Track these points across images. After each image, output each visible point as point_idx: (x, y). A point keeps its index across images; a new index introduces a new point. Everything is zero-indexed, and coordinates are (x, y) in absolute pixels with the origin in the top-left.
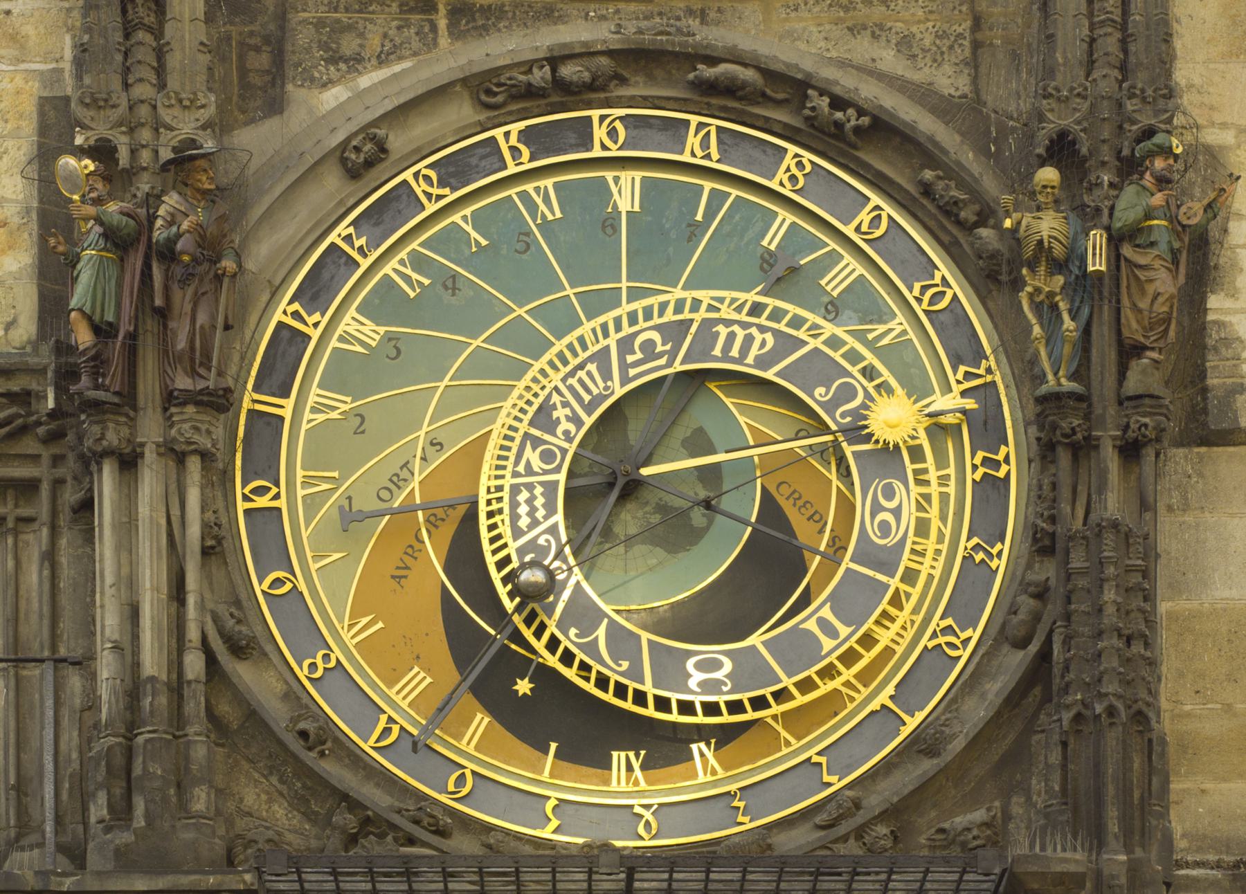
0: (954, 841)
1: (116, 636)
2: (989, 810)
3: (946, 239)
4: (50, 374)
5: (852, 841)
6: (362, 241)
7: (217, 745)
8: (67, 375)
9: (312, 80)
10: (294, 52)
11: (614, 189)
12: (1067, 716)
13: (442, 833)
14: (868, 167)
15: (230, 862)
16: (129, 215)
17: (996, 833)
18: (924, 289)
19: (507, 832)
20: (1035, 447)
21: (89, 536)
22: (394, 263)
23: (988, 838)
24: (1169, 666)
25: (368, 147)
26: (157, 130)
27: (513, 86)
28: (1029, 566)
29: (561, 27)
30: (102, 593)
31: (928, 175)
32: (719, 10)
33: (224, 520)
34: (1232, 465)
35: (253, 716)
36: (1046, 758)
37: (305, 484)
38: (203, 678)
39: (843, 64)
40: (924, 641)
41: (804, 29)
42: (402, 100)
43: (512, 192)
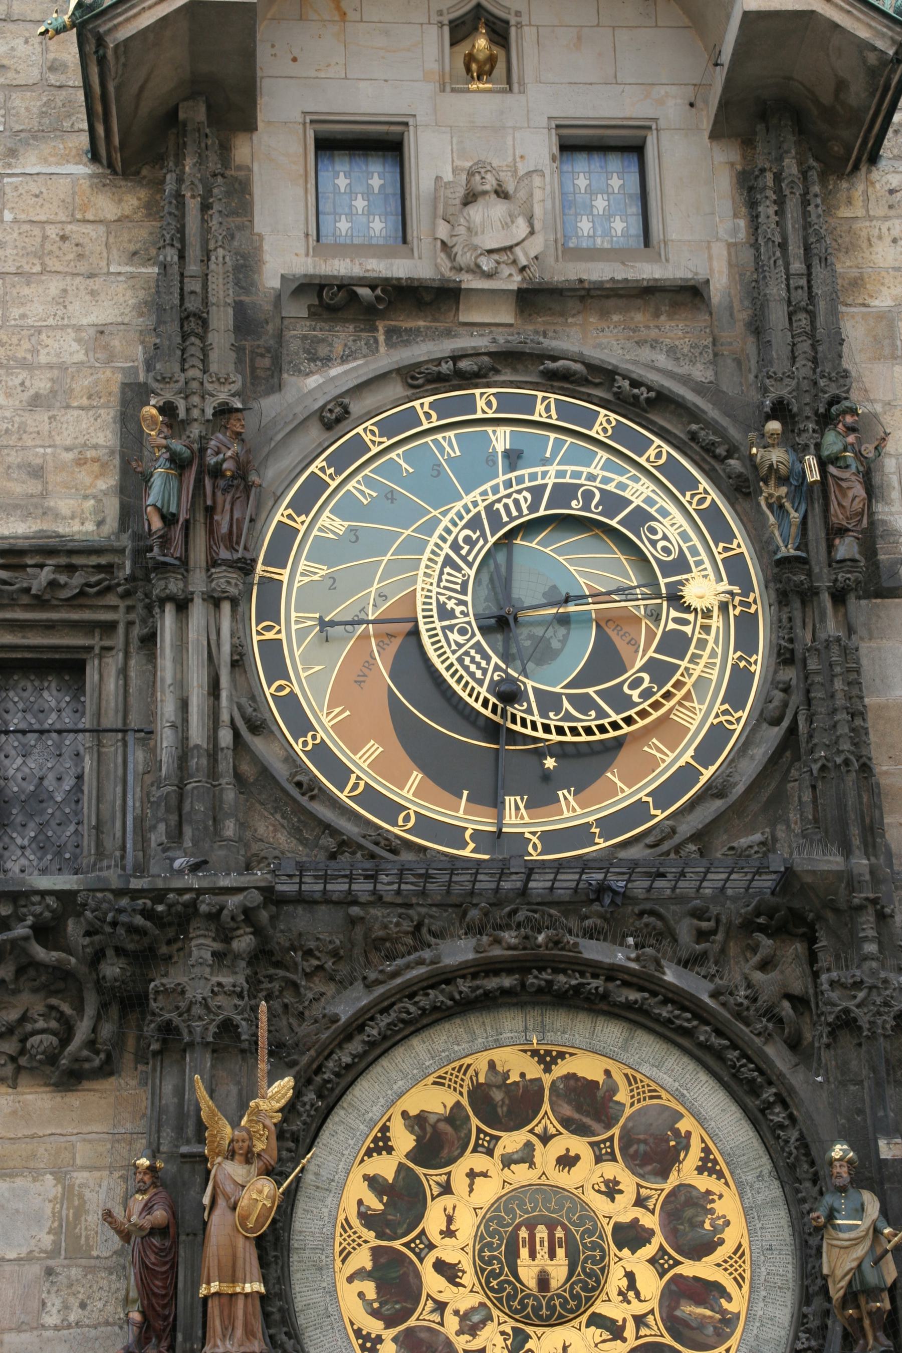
3: (706, 467)
5: (672, 856)
6: (332, 470)
8: (140, 553)
9: (300, 371)
13: (394, 851)
18: (693, 496)
21: (152, 658)
24: (873, 737)
28: (776, 672)
30: (163, 692)
31: (694, 427)
34: (899, 611)
35: (265, 772)
36: (800, 798)
37: (297, 622)
39: (635, 363)
40: (711, 720)
43: (428, 439)
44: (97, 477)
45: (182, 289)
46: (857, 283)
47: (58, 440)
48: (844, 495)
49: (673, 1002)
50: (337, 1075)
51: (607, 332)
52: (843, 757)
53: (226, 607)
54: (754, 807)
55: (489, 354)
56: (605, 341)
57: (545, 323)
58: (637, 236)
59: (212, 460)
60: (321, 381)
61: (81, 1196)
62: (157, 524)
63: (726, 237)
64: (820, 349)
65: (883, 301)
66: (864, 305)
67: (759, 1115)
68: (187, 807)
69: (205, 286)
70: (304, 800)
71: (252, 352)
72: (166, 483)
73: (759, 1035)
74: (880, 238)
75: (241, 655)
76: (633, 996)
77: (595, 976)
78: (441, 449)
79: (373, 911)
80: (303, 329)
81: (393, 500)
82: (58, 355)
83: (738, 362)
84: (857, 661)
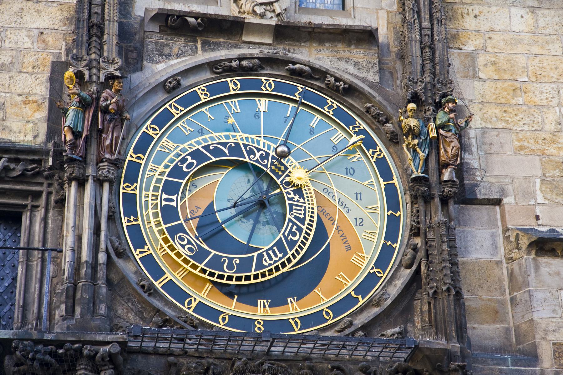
1: (73, 246)
2: (400, 328)
3: (374, 127)
4: (51, 153)
7: (110, 290)
9: (153, 61)
10: (147, 51)
11: (259, 104)
14: (347, 102)
22: (181, 123)
27: (225, 66)
28: (409, 240)
31: (368, 105)
32: (294, 50)
33: (115, 206)
35: (124, 278)
41: (323, 58)
43: (223, 102)
44: (35, 111)
46: (455, 37)
47: (13, 89)
48: (449, 146)
51: (322, 52)
52: (447, 286)
53: (106, 186)
54: (396, 313)
55: (259, 58)
56: (321, 56)
57: (289, 45)
58: (339, 5)
60: (165, 67)
62: (69, 137)
63: (386, 8)
65: (469, 47)
66: (459, 49)
68: (78, 296)
70: (145, 296)
71: (126, 49)
72: (76, 115)
74: (468, 14)
75: (114, 212)
78: (230, 108)
80: (156, 38)
82: (16, 43)
84: (454, 236)
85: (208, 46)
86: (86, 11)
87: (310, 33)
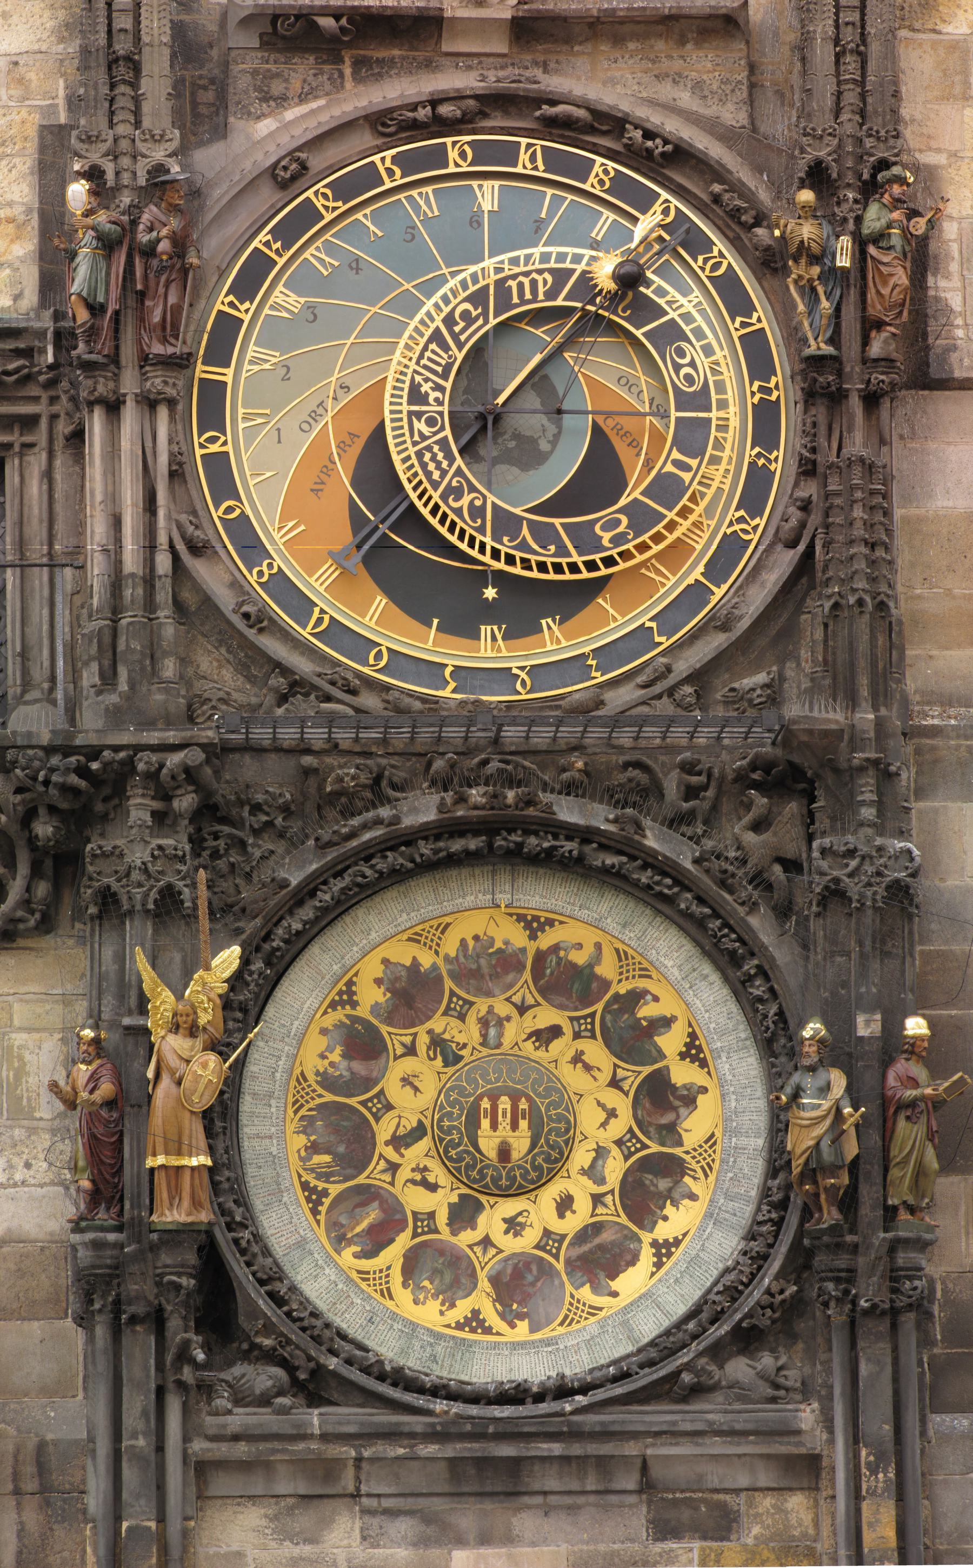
0: (742, 698)
3: (731, 235)
5: (665, 698)
12: (828, 605)
13: (353, 692)
15: (191, 719)
16: (114, 223)
17: (773, 695)
19: (402, 691)
20: (799, 393)
23: (768, 696)
25: (294, 166)
26: (135, 157)
28: (796, 484)
29: (439, 76)
31: (717, 188)
35: (207, 602)
38: (170, 573)
42: (320, 131)
45: (110, 25)
48: (885, 283)
49: (653, 867)
50: (286, 942)
51: (620, 64)
53: (163, 413)
54: (762, 642)
56: (618, 74)
57: (546, 52)
59: (144, 238)
61: (21, 1058)
62: (83, 315)
64: (870, 100)
67: (739, 986)
68: (121, 646)
69: (137, 21)
70: (251, 633)
72: (93, 269)
73: (743, 904)
75: (181, 464)
76: (611, 860)
77: (569, 838)
78: (417, 208)
79: (328, 760)
81: (358, 270)
83: (780, 94)
85: (367, 70)
86: (102, 29)
87: (591, 25)
